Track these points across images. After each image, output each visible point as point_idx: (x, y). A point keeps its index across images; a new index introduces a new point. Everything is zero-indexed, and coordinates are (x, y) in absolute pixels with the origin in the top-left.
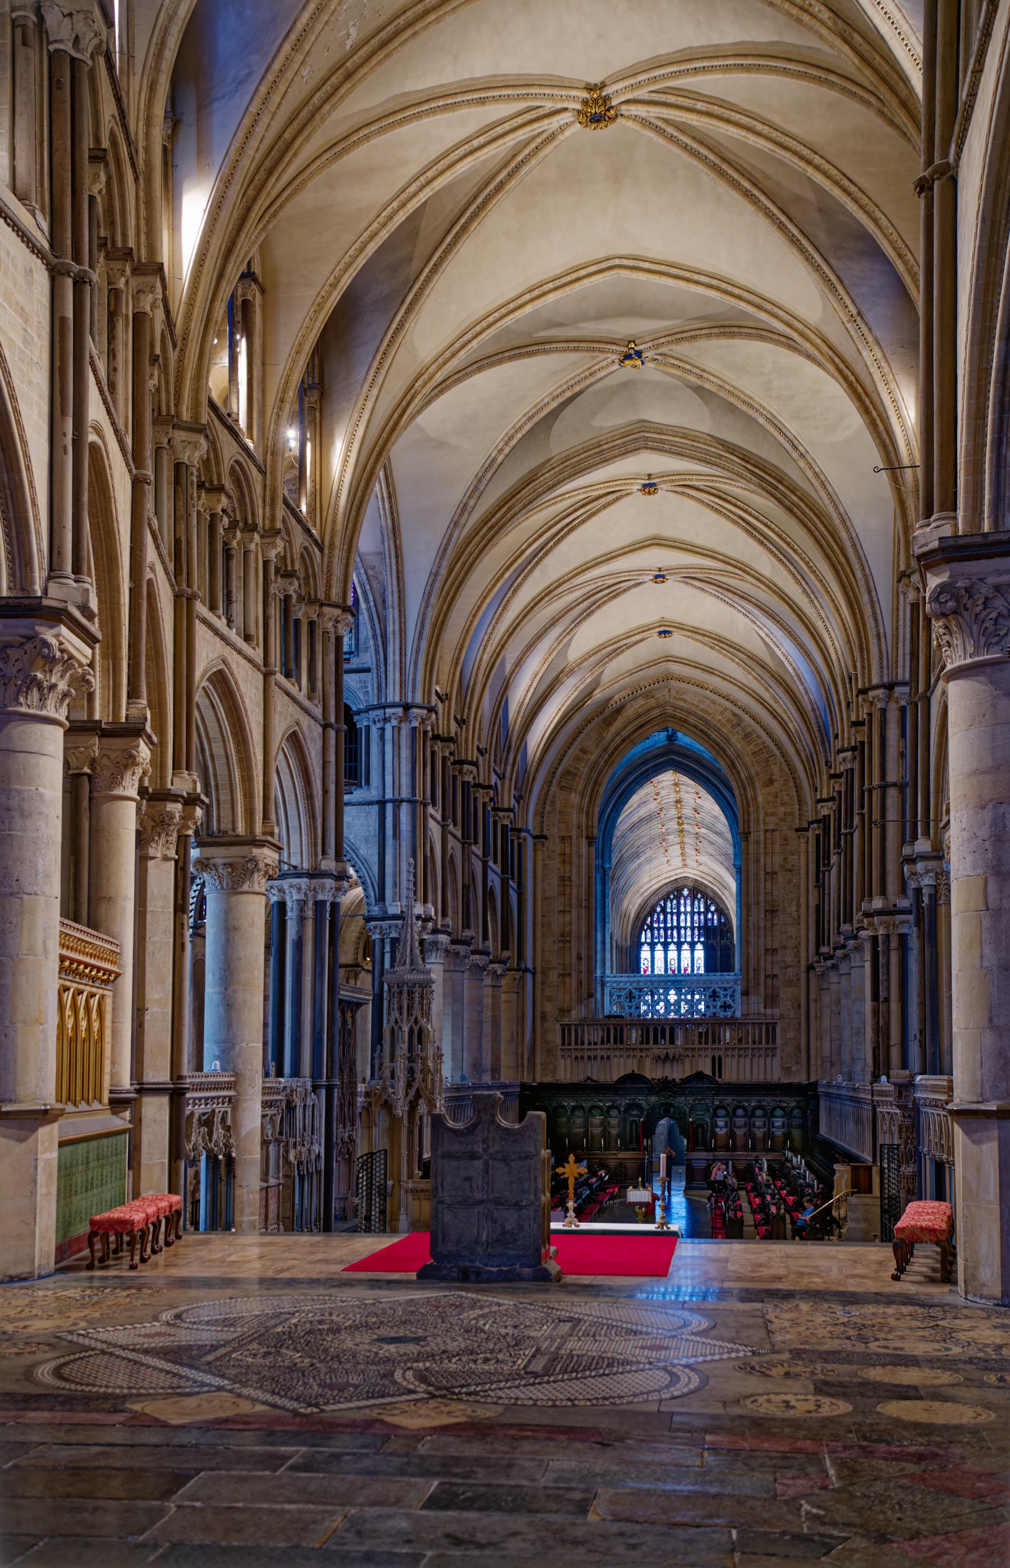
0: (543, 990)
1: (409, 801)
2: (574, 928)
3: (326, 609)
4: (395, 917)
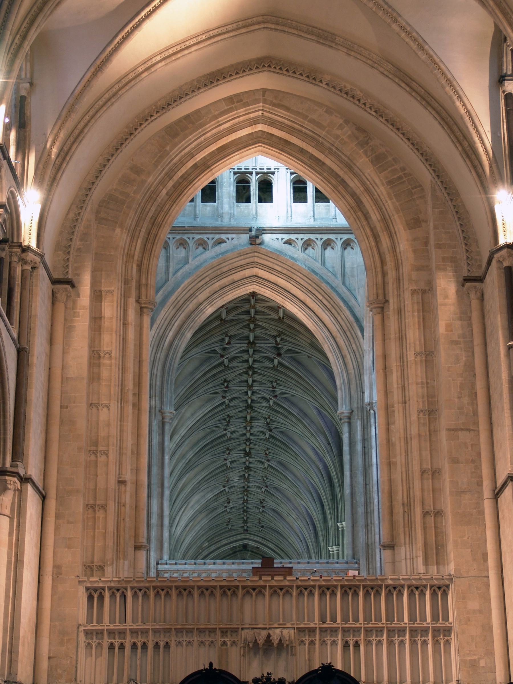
0: (57, 528)
2: (114, 431)
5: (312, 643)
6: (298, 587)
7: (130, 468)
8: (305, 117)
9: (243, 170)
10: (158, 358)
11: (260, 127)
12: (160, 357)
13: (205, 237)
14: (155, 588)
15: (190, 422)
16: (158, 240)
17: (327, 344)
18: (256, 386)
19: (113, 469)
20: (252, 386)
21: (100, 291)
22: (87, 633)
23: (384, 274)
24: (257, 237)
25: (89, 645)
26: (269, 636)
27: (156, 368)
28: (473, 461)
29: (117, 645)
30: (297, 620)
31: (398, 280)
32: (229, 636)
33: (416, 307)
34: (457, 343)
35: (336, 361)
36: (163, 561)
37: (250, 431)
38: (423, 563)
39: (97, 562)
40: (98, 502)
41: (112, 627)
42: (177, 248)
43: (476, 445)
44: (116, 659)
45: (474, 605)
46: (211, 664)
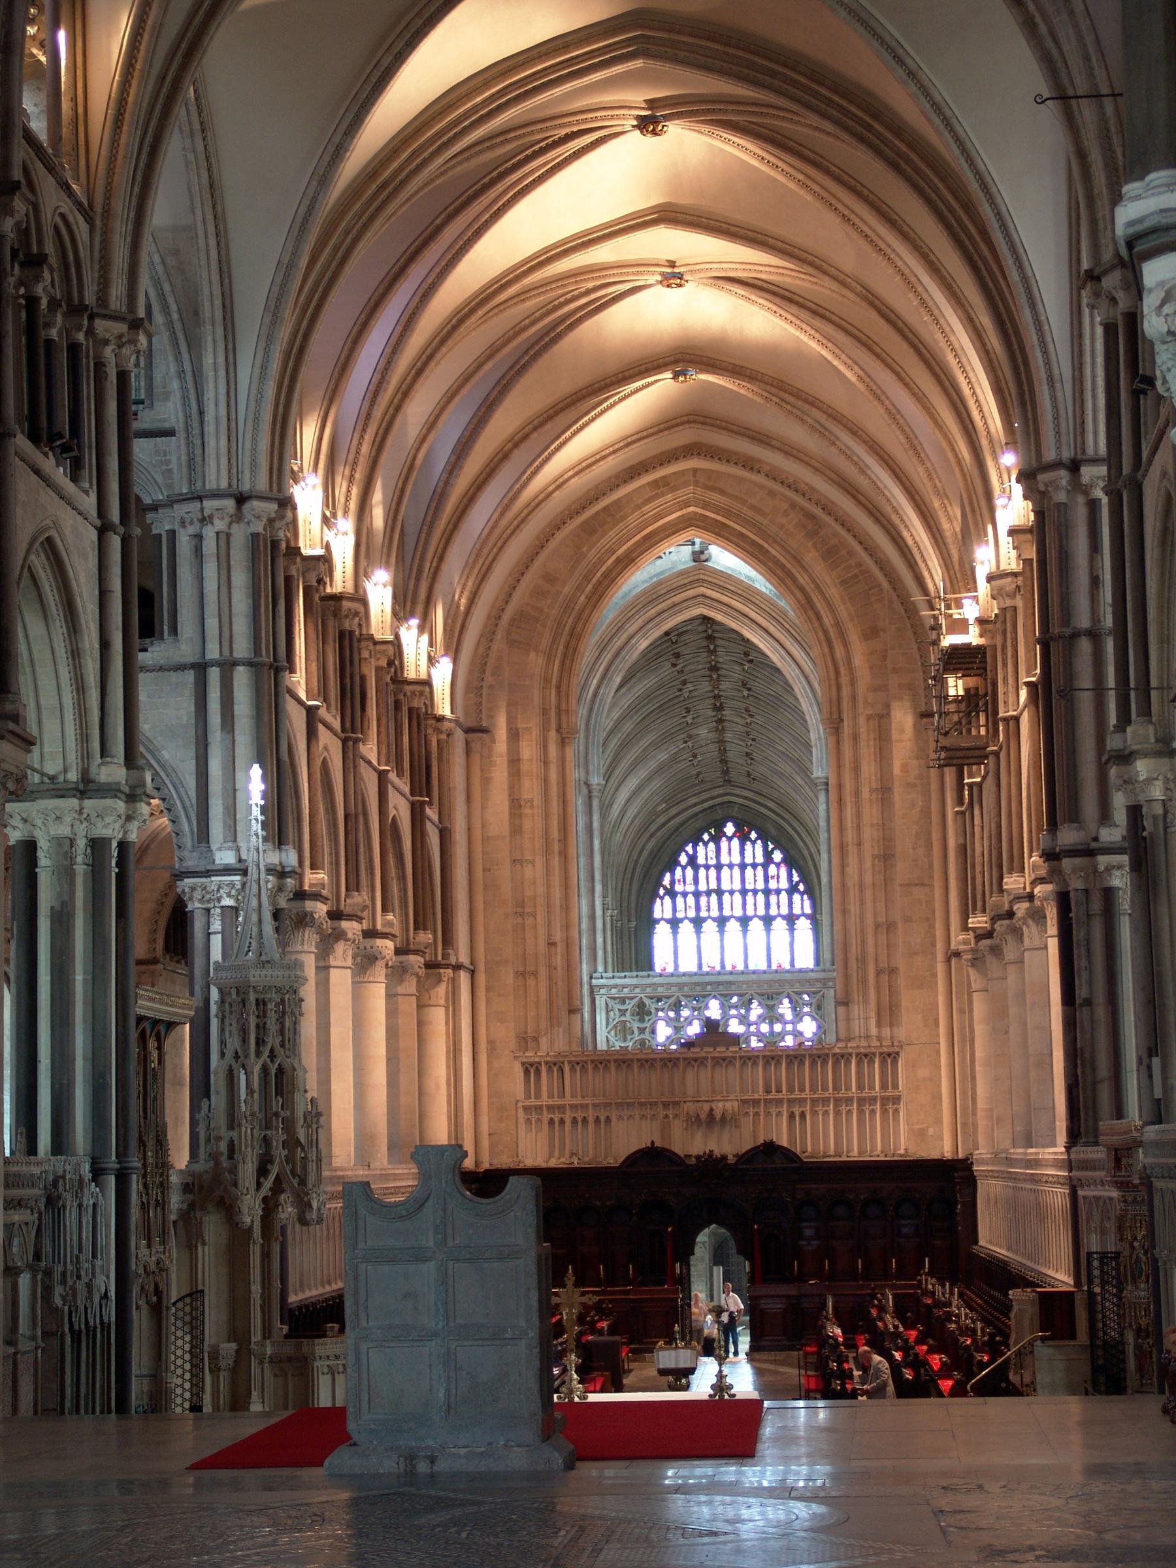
0: (488, 1001)
1: (250, 664)
2: (541, 890)
3: (100, 325)
4: (227, 870)
5: (756, 1114)
6: (741, 1058)
8: (744, 502)
11: (691, 509)
14: (592, 1061)
19: (542, 932)
21: (517, 729)
22: (526, 1108)
23: (839, 688)
24: (702, 552)
25: (528, 1121)
26: (712, 1110)
28: (927, 919)
29: (557, 1120)
30: (742, 1092)
31: (854, 697)
33: (872, 736)
34: (913, 786)
36: (598, 975)
39: (531, 1034)
40: (528, 969)
41: (551, 1102)
43: (930, 902)
44: (557, 1134)
45: (923, 1073)
46: (653, 1143)
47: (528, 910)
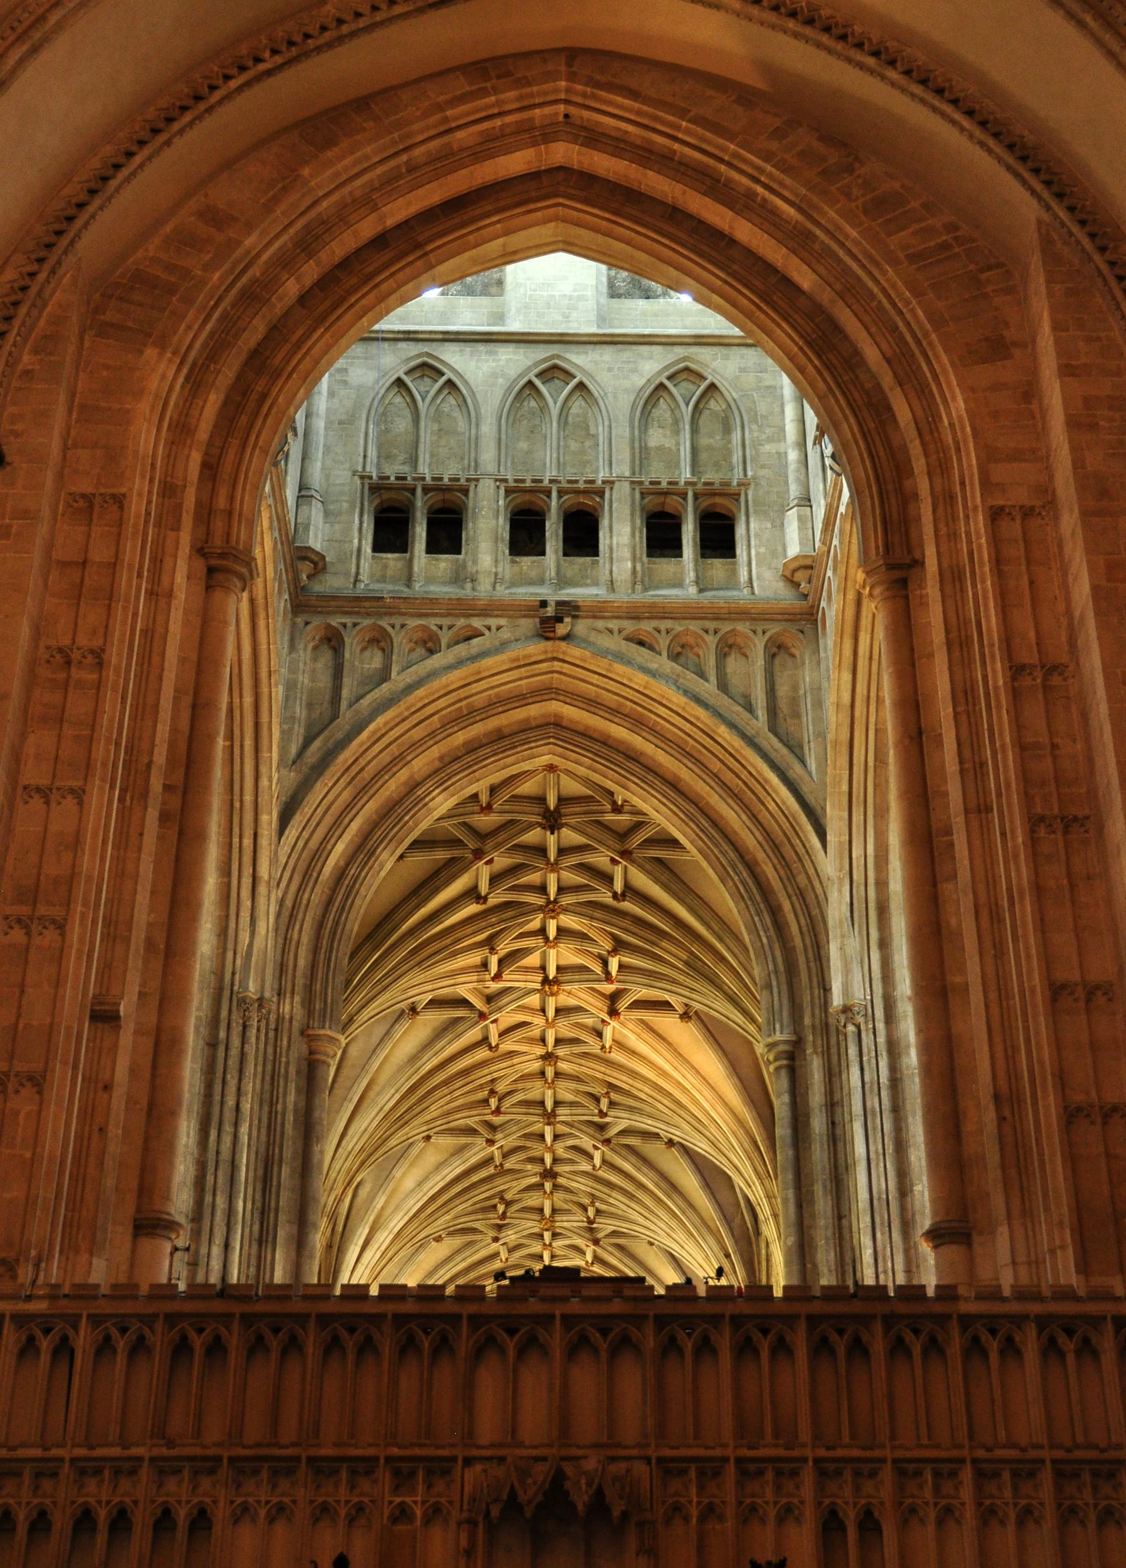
7: (137, 989)
9: (528, 484)
10: (304, 902)
12: (309, 901)
13: (432, 623)
15: (412, 1202)
16: (270, 408)
17: (732, 879)
18: (563, 1113)
20: (553, 1114)
27: (297, 927)
32: (421, 1488)
35: (756, 919)
37: (550, 1245)
38: (1076, 1265)
42: (364, 649)
47: (42, 910)
